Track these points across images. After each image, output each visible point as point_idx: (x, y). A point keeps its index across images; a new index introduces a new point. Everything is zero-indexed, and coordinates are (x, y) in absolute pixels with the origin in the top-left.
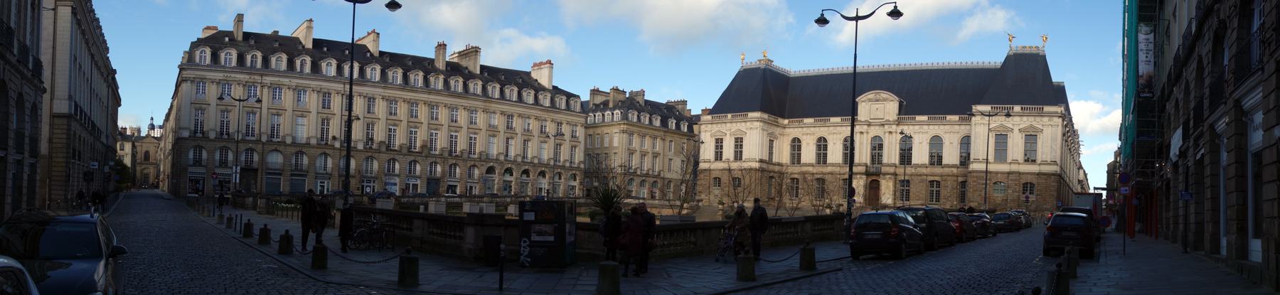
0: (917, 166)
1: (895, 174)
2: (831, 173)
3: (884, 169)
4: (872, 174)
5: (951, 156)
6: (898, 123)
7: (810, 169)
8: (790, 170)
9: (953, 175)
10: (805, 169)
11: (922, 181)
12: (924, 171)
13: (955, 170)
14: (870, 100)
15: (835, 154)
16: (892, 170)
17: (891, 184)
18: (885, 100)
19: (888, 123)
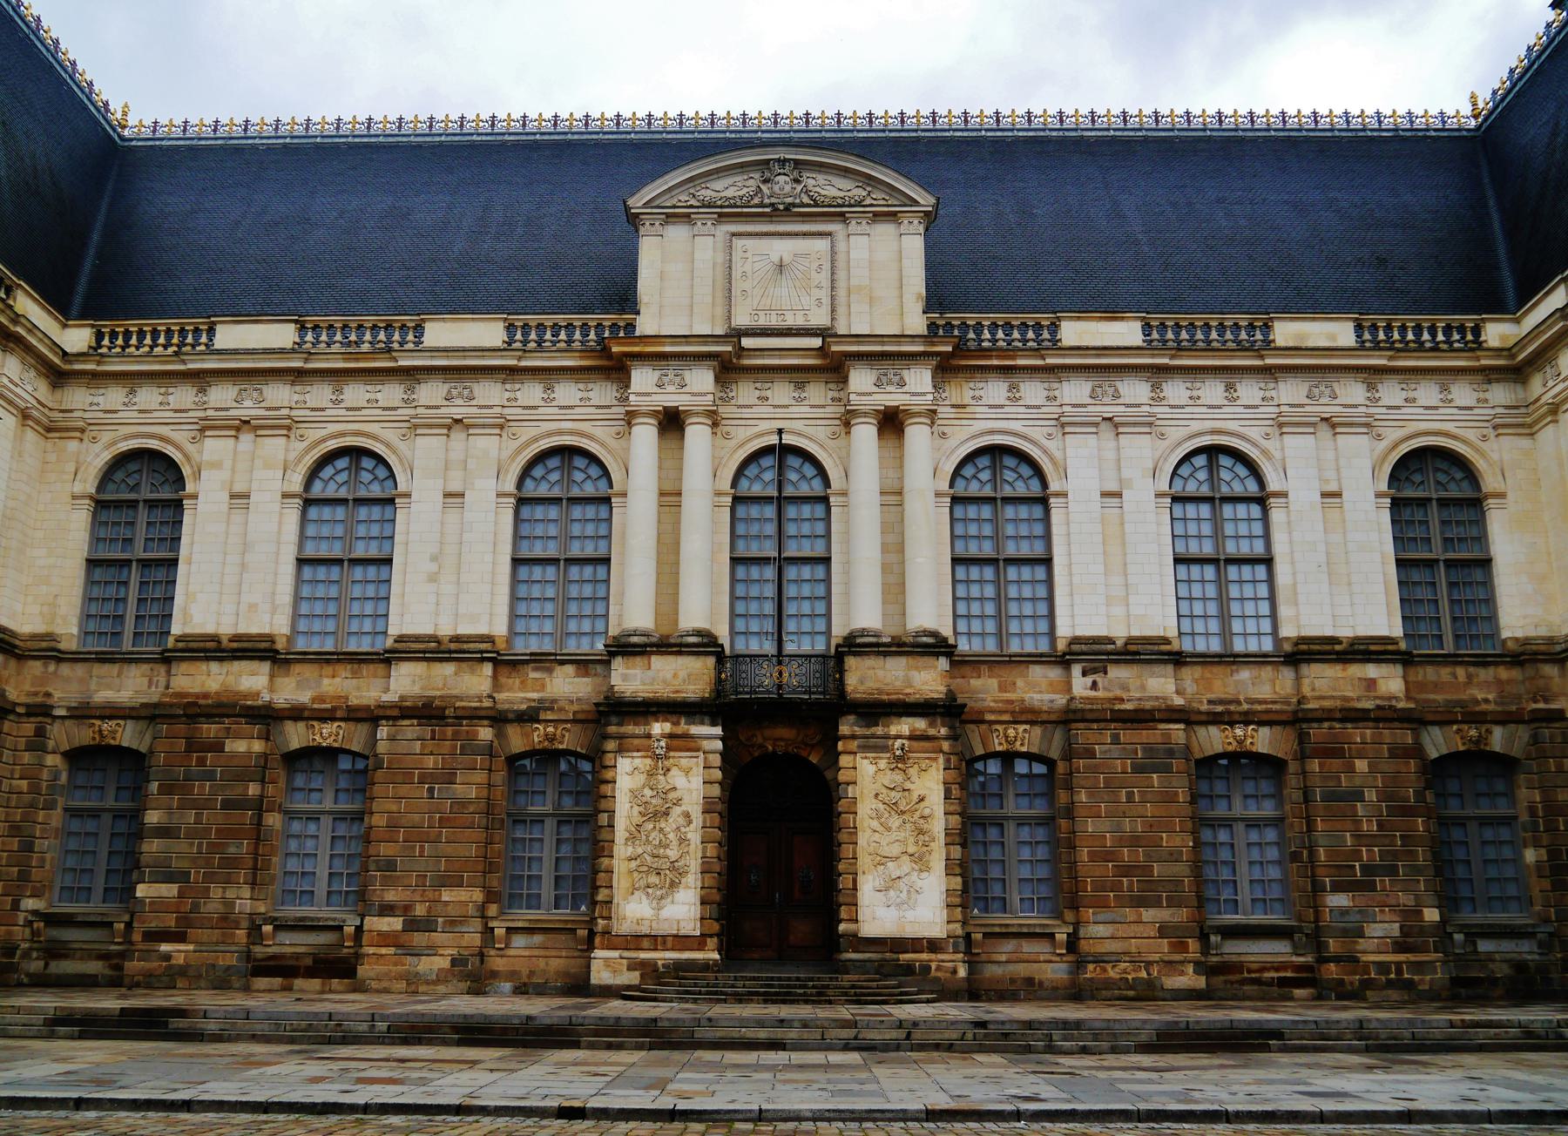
0: (1095, 654)
1: (949, 710)
2: (427, 712)
3: (863, 677)
4: (778, 709)
5: (1338, 574)
6: (954, 361)
7: (252, 680)
8: (66, 687)
9: (1385, 715)
10: (209, 679)
11: (1156, 760)
12: (1160, 685)
13: (1390, 681)
14: (726, 213)
15: (452, 571)
16: (928, 680)
17: (930, 783)
18: (839, 213)
19: (887, 356)
